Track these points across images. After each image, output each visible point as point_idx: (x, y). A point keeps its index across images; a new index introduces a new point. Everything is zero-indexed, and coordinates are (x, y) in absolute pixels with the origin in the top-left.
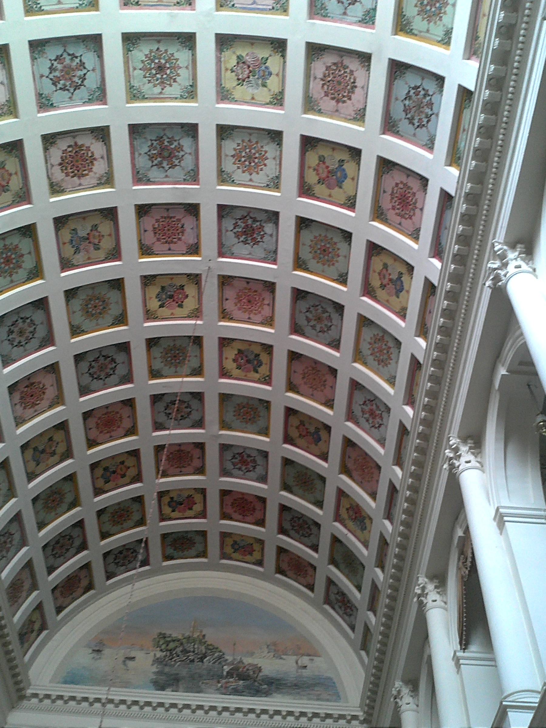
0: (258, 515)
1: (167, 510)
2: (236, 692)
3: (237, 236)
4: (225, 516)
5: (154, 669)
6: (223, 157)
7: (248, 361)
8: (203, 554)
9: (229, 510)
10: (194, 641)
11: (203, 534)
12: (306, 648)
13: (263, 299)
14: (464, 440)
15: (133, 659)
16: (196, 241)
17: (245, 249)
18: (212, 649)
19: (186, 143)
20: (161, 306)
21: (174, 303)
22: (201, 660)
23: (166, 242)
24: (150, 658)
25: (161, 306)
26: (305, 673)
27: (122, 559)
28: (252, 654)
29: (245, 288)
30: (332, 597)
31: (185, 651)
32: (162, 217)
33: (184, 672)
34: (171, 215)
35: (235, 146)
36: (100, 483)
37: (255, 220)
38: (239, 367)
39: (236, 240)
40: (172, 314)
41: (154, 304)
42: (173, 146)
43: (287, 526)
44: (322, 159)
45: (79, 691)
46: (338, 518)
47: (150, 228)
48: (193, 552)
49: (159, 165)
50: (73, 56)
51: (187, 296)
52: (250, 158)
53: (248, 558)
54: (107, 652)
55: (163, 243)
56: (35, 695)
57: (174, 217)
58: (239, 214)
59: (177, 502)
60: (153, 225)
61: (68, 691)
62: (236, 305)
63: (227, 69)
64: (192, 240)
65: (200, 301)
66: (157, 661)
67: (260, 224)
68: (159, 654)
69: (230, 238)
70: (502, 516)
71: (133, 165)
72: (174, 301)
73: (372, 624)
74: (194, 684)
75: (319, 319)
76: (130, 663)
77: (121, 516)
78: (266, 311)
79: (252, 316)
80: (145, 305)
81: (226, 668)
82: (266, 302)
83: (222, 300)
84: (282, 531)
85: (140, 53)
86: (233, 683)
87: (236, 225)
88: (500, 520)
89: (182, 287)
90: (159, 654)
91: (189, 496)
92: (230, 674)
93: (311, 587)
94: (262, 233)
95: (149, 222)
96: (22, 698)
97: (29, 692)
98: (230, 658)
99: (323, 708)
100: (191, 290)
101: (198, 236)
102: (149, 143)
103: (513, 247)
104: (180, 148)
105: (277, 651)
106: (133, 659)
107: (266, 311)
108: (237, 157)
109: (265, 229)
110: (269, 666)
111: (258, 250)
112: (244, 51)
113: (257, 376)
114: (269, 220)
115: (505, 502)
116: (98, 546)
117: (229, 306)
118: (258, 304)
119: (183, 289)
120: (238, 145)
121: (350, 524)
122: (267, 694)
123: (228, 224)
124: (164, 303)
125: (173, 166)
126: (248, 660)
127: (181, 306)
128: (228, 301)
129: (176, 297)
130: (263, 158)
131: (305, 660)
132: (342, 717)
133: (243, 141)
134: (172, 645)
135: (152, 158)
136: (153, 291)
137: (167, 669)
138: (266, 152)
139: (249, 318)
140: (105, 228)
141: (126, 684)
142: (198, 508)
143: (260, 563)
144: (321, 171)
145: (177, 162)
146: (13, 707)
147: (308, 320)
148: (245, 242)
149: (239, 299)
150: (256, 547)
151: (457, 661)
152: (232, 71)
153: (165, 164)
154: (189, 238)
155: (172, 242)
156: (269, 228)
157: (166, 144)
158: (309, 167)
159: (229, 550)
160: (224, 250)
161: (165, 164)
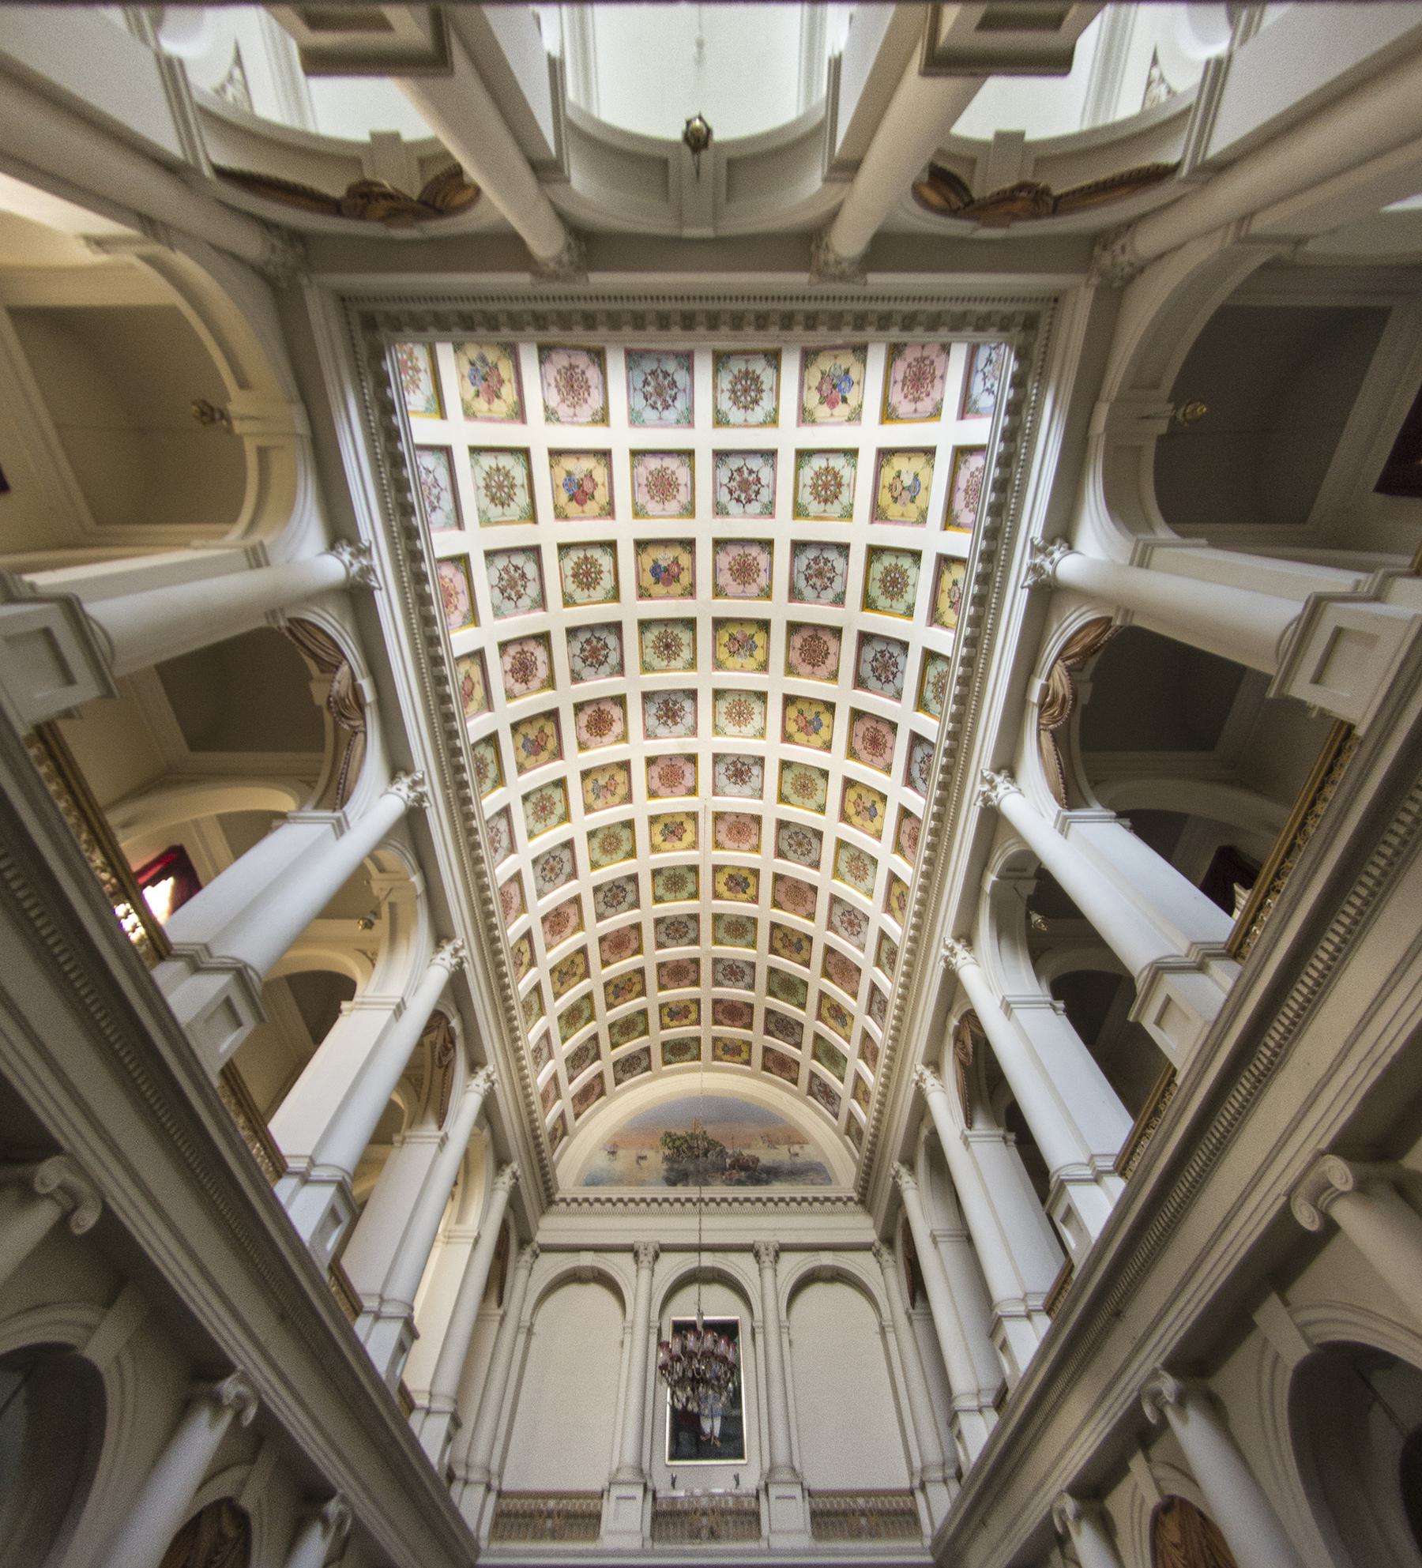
0: (746, 1020)
1: (667, 1020)
2: (740, 1183)
4: (716, 1022)
5: (665, 1166)
7: (738, 884)
8: (698, 1058)
9: (720, 1017)
10: (697, 1138)
11: (698, 1040)
12: (794, 1137)
14: (957, 939)
15: (644, 1158)
17: (735, 789)
18: (713, 1144)
19: (687, 705)
22: (705, 1154)
24: (660, 1157)
26: (798, 1160)
27: (630, 1066)
28: (749, 1146)
30: (815, 1089)
31: (690, 1148)
33: (691, 1168)
36: (611, 999)
38: (730, 889)
41: (658, 839)
43: (772, 1027)
44: (801, 712)
45: (603, 1192)
46: (819, 1017)
47: (656, 775)
48: (688, 1056)
49: (665, 723)
50: (599, 639)
52: (740, 714)
53: (737, 1058)
54: (621, 1153)
56: (563, 1200)
58: (729, 760)
59: (675, 1013)
61: (592, 1193)
65: (697, 834)
66: (667, 1159)
68: (667, 1152)
69: (723, 780)
70: (1008, 1004)
74: (703, 1180)
76: (642, 1162)
77: (628, 1028)
78: (754, 840)
81: (728, 1161)
83: (716, 832)
84: (768, 1032)
85: (651, 636)
86: (737, 1175)
87: (727, 769)
88: (1007, 1008)
89: (682, 823)
90: (667, 1152)
91: (686, 1007)
92: (732, 1167)
93: (795, 1082)
95: (656, 770)
96: (551, 1202)
97: (557, 1197)
98: (730, 1152)
99: (810, 1191)
100: (689, 826)
101: (696, 780)
103: (998, 772)
104: (682, 708)
105: (772, 1142)
106: (644, 1158)
107: (754, 840)
108: (729, 714)
110: (766, 1156)
112: (735, 630)
113: (745, 896)
114: (756, 763)
115: (1007, 992)
116: (611, 1055)
117: (722, 837)
121: (832, 1022)
122: (767, 1182)
123: (721, 768)
125: (676, 723)
126: (746, 1152)
130: (751, 714)
131: (796, 1148)
132: (839, 1199)
134: (678, 1143)
135: (659, 718)
137: (676, 1166)
140: (620, 777)
141: (641, 1183)
142: (693, 1016)
143: (748, 1062)
146: (543, 1213)
147: (790, 845)
149: (730, 831)
150: (744, 1048)
151: (966, 1141)
154: (688, 781)
159: (720, 1052)
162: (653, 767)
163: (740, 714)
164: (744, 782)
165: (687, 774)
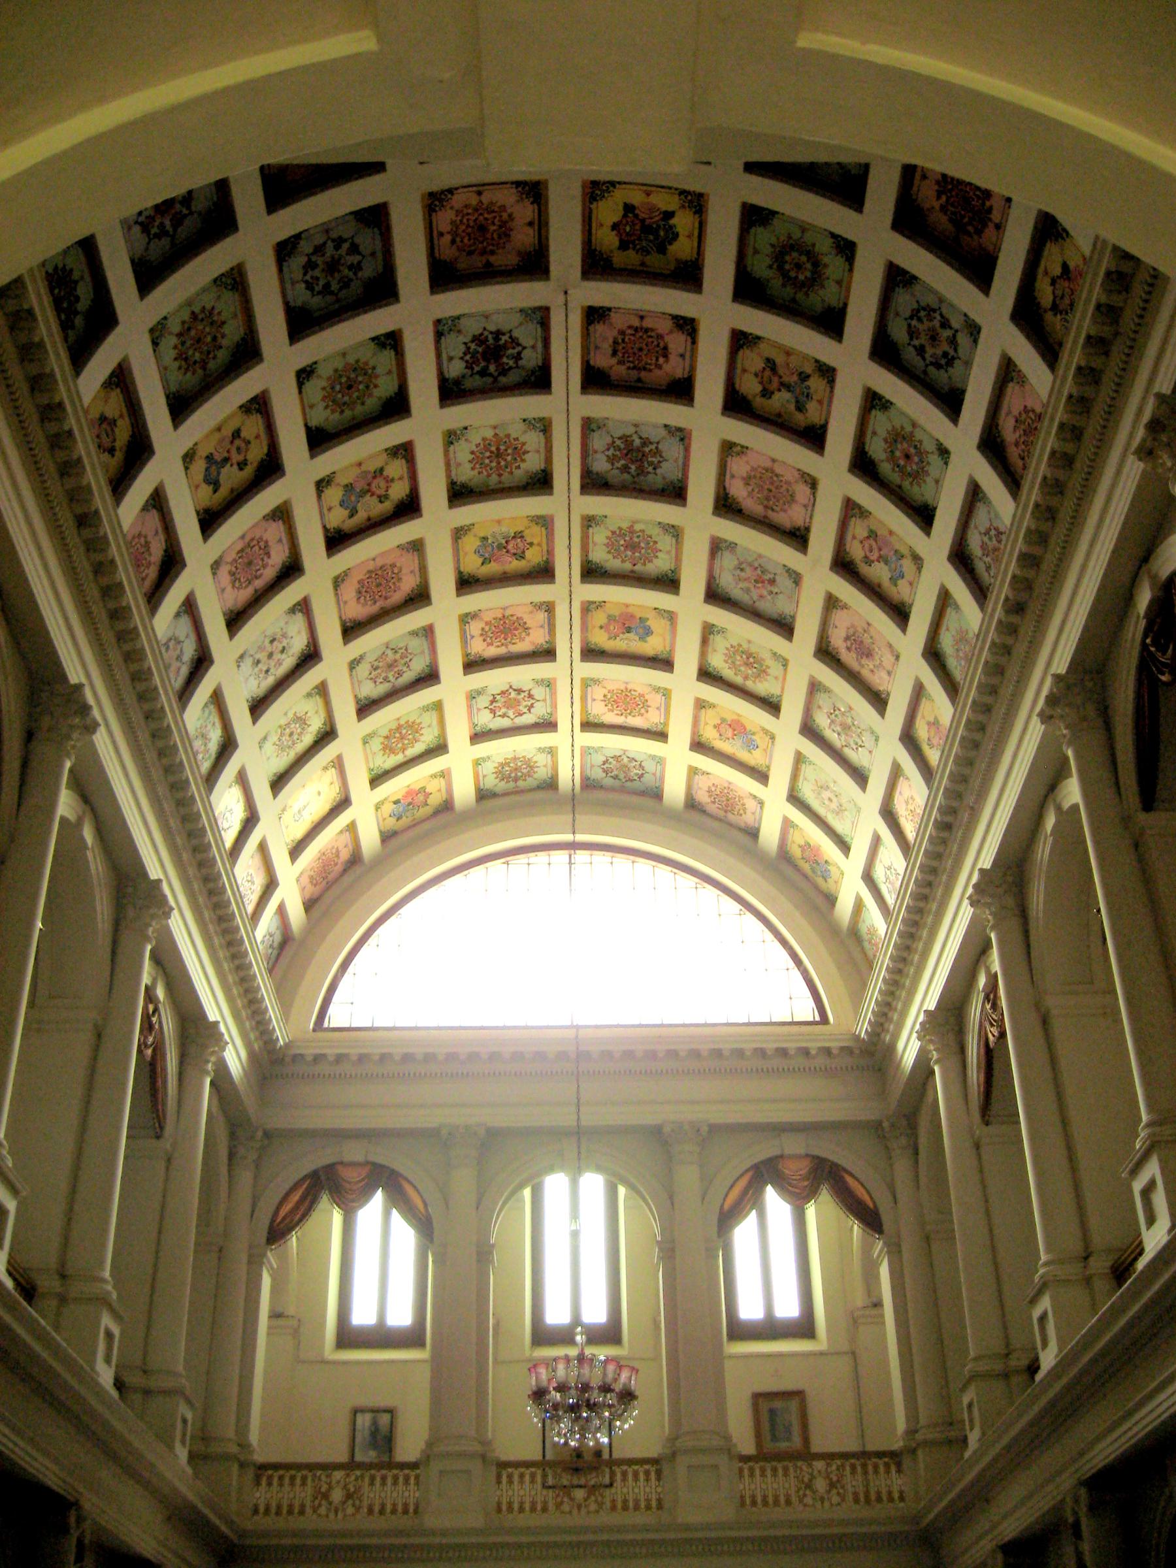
3: (515, 342)
6: (542, 450)
13: (453, 242)
16: (591, 328)
20: (669, 215)
21: (642, 216)
23: (647, 330)
25: (669, 215)
29: (492, 253)
32: (650, 370)
34: (635, 372)
35: (523, 465)
37: (483, 373)
39: (515, 334)
40: (648, 194)
41: (683, 222)
42: (623, 462)
49: (646, 442)
51: (615, 227)
55: (652, 330)
57: (629, 368)
58: (512, 378)
60: (667, 361)
62: (510, 216)
63: (539, 545)
64: (599, 329)
65: (588, 219)
67: (472, 369)
69: (527, 335)
71: (687, 450)
72: (643, 221)
73: (219, 840)
75: (332, 267)
78: (445, 219)
79: (474, 201)
80: (702, 225)
82: (447, 238)
83: (541, 224)
87: (518, 357)
89: (623, 246)
94: (468, 357)
95: (674, 368)
100: (607, 239)
102: (658, 471)
104: (612, 460)
107: (445, 219)
109: (463, 365)
111: (472, 328)
114: (457, 382)
117: (525, 211)
118: (464, 227)
119: (621, 241)
120: (518, 467)
124: (662, 219)
127: (629, 208)
128: (528, 220)
129: (637, 227)
133: (511, 473)
136: (682, 248)
138: (473, 469)
139: (479, 193)
144: (383, 484)
145: (618, 442)
148: (498, 334)
149: (505, 231)
152: (531, 544)
153: (637, 442)
155: (636, 329)
156: (456, 369)
157: (633, 467)
158: (401, 478)
160: (539, 315)
161: (637, 442)
162: (679, 373)
163: (499, 455)
164: (478, 339)
165: (607, 347)
